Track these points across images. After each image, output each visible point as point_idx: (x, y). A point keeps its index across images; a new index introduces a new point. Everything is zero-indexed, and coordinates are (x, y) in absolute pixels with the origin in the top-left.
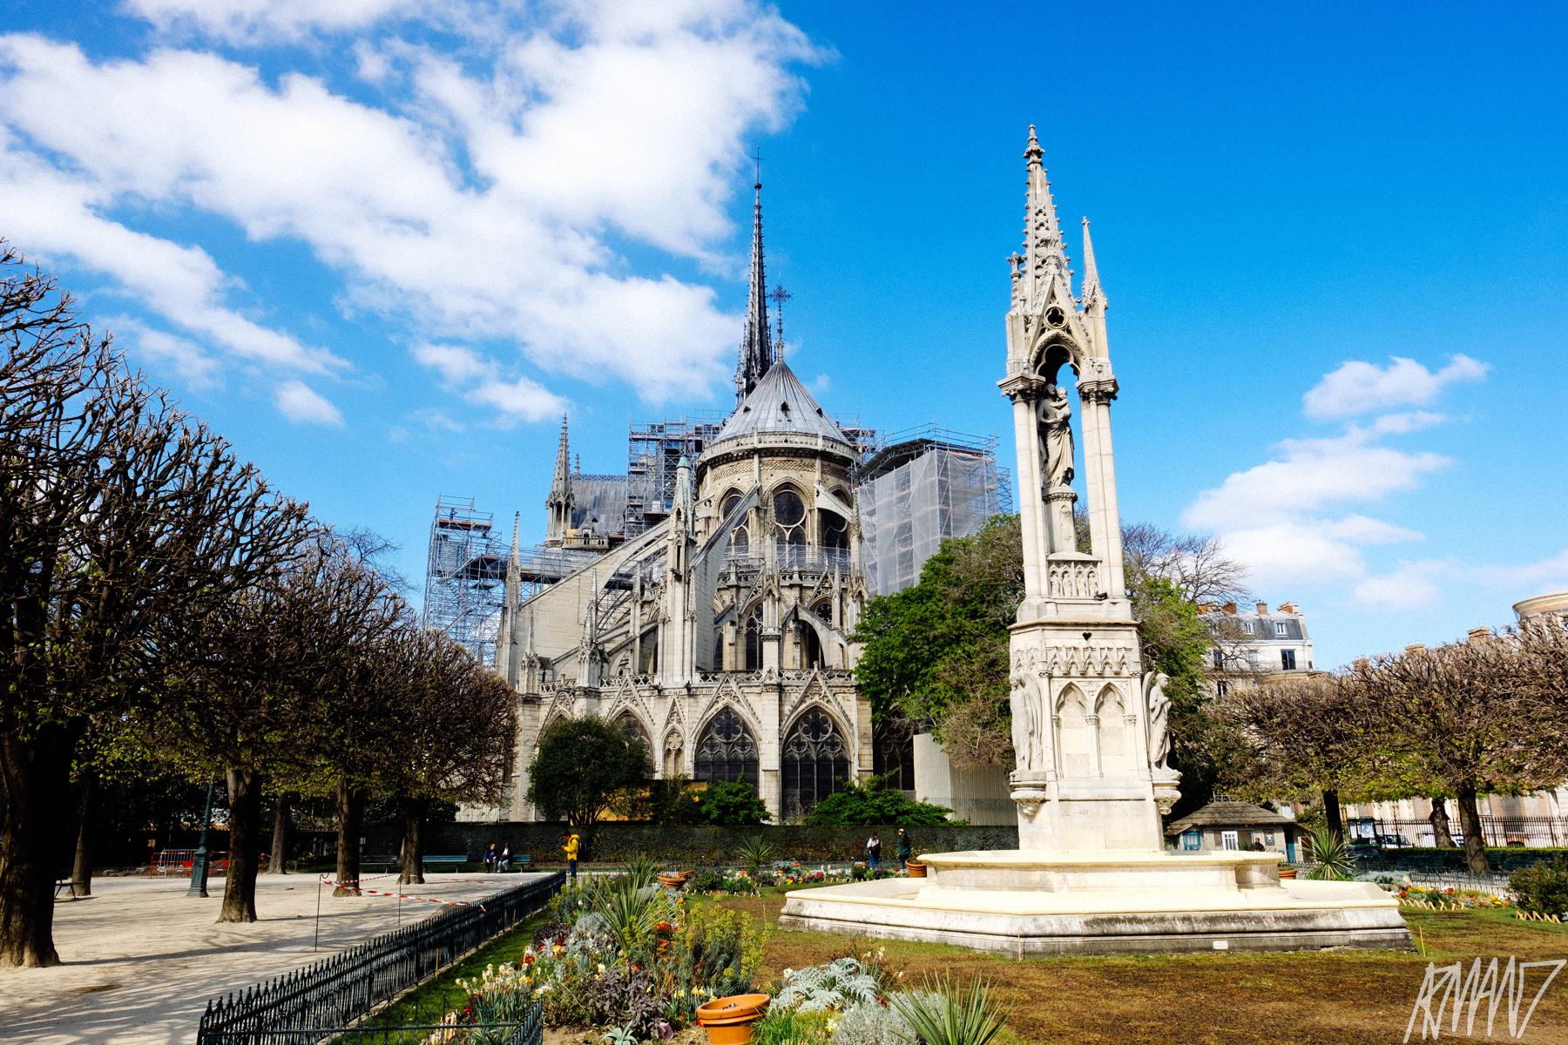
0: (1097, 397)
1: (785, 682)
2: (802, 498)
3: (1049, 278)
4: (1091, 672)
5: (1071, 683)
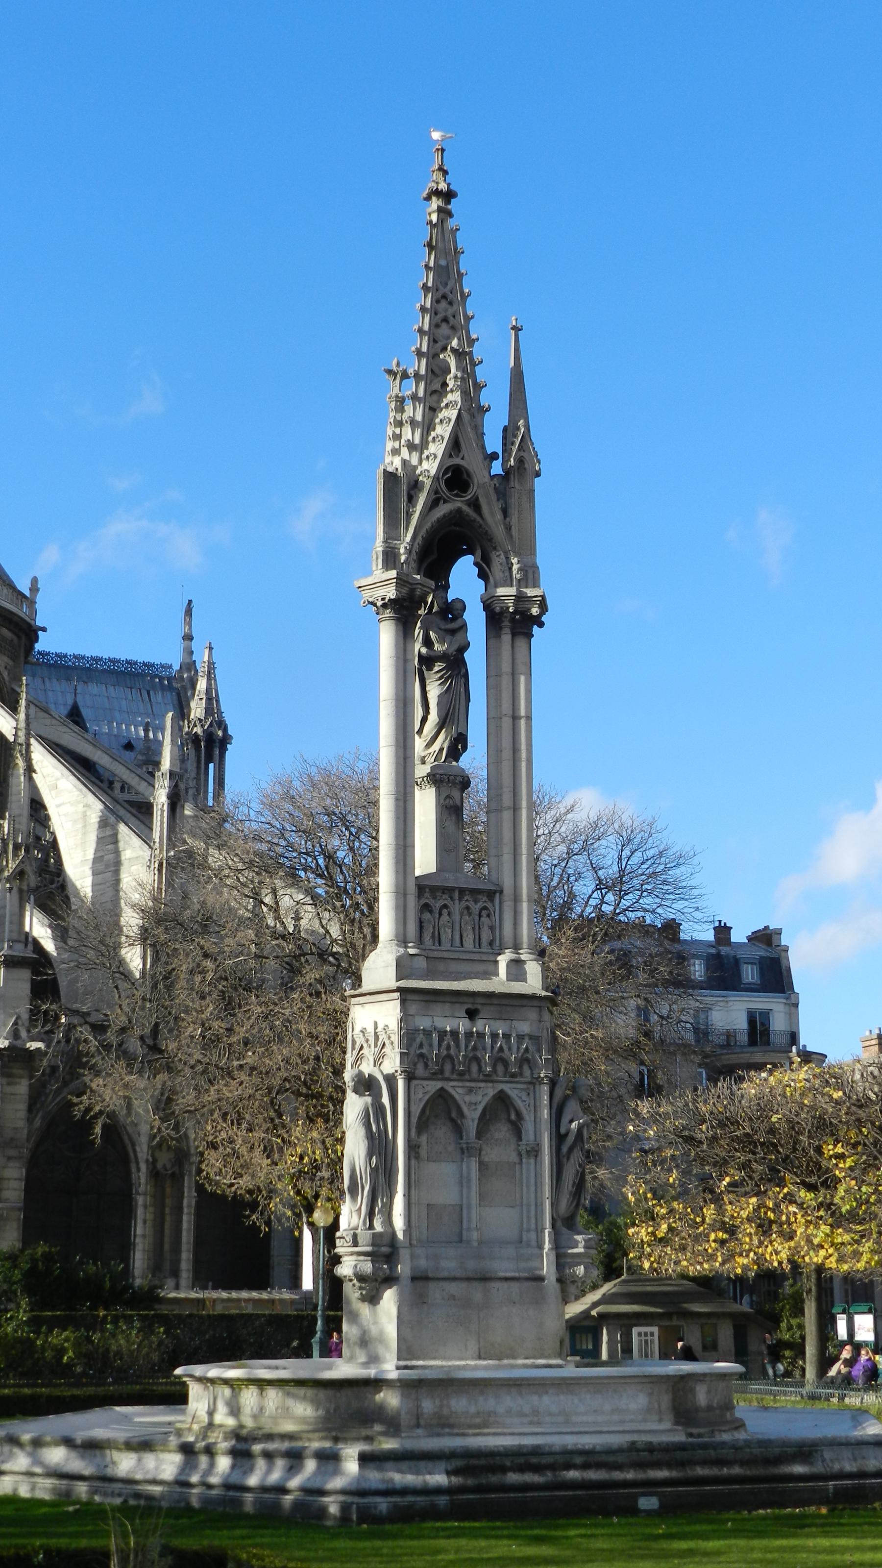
0: (513, 620)
5: (442, 1089)
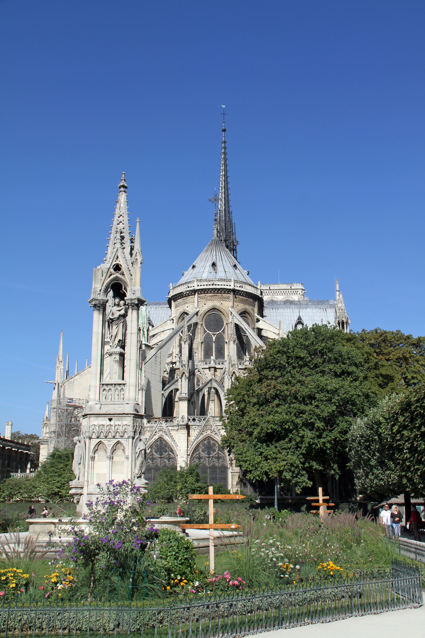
2: (222, 316)
3: (115, 250)
4: (110, 436)
5: (101, 441)
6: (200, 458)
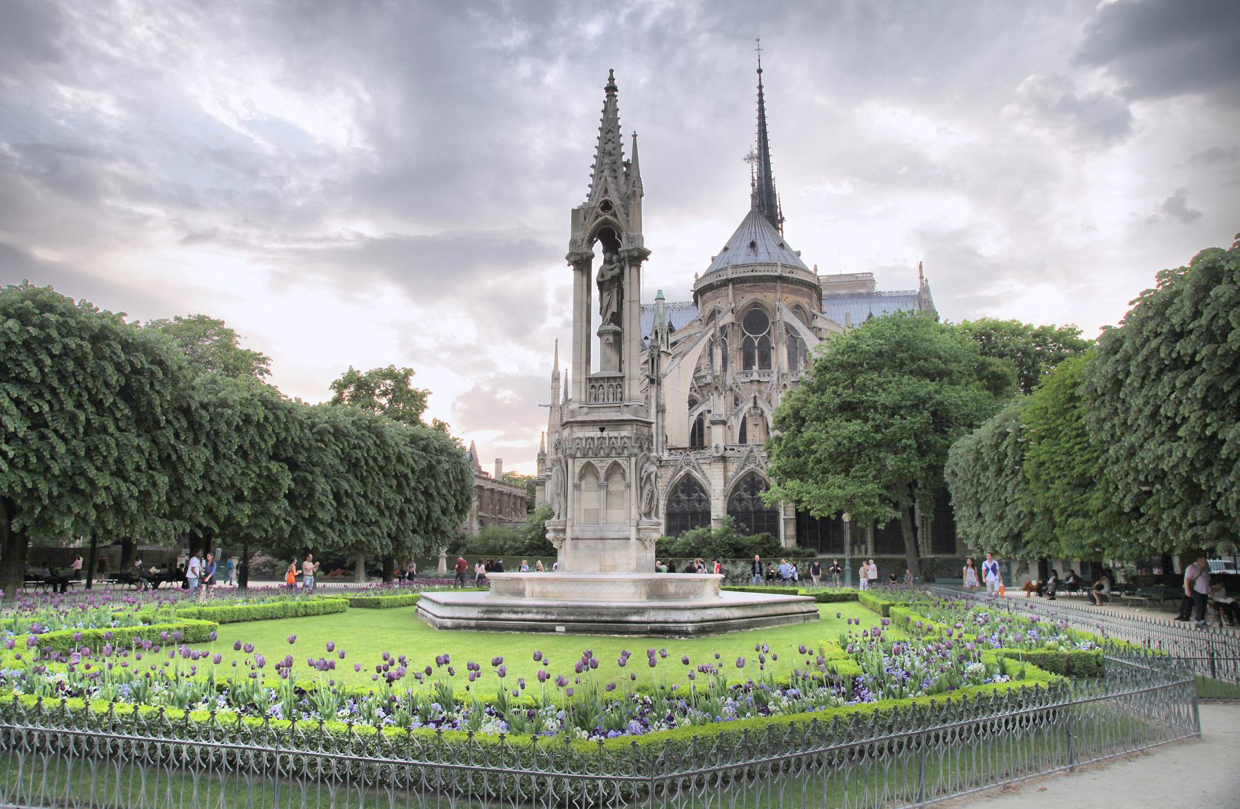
1: (729, 453)
3: (603, 179)
6: (741, 500)
